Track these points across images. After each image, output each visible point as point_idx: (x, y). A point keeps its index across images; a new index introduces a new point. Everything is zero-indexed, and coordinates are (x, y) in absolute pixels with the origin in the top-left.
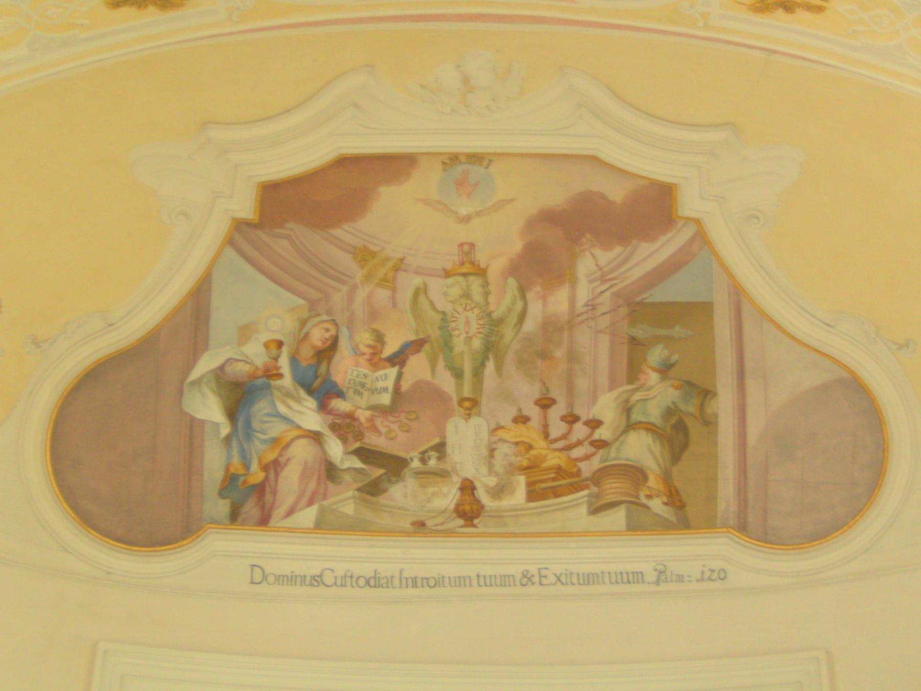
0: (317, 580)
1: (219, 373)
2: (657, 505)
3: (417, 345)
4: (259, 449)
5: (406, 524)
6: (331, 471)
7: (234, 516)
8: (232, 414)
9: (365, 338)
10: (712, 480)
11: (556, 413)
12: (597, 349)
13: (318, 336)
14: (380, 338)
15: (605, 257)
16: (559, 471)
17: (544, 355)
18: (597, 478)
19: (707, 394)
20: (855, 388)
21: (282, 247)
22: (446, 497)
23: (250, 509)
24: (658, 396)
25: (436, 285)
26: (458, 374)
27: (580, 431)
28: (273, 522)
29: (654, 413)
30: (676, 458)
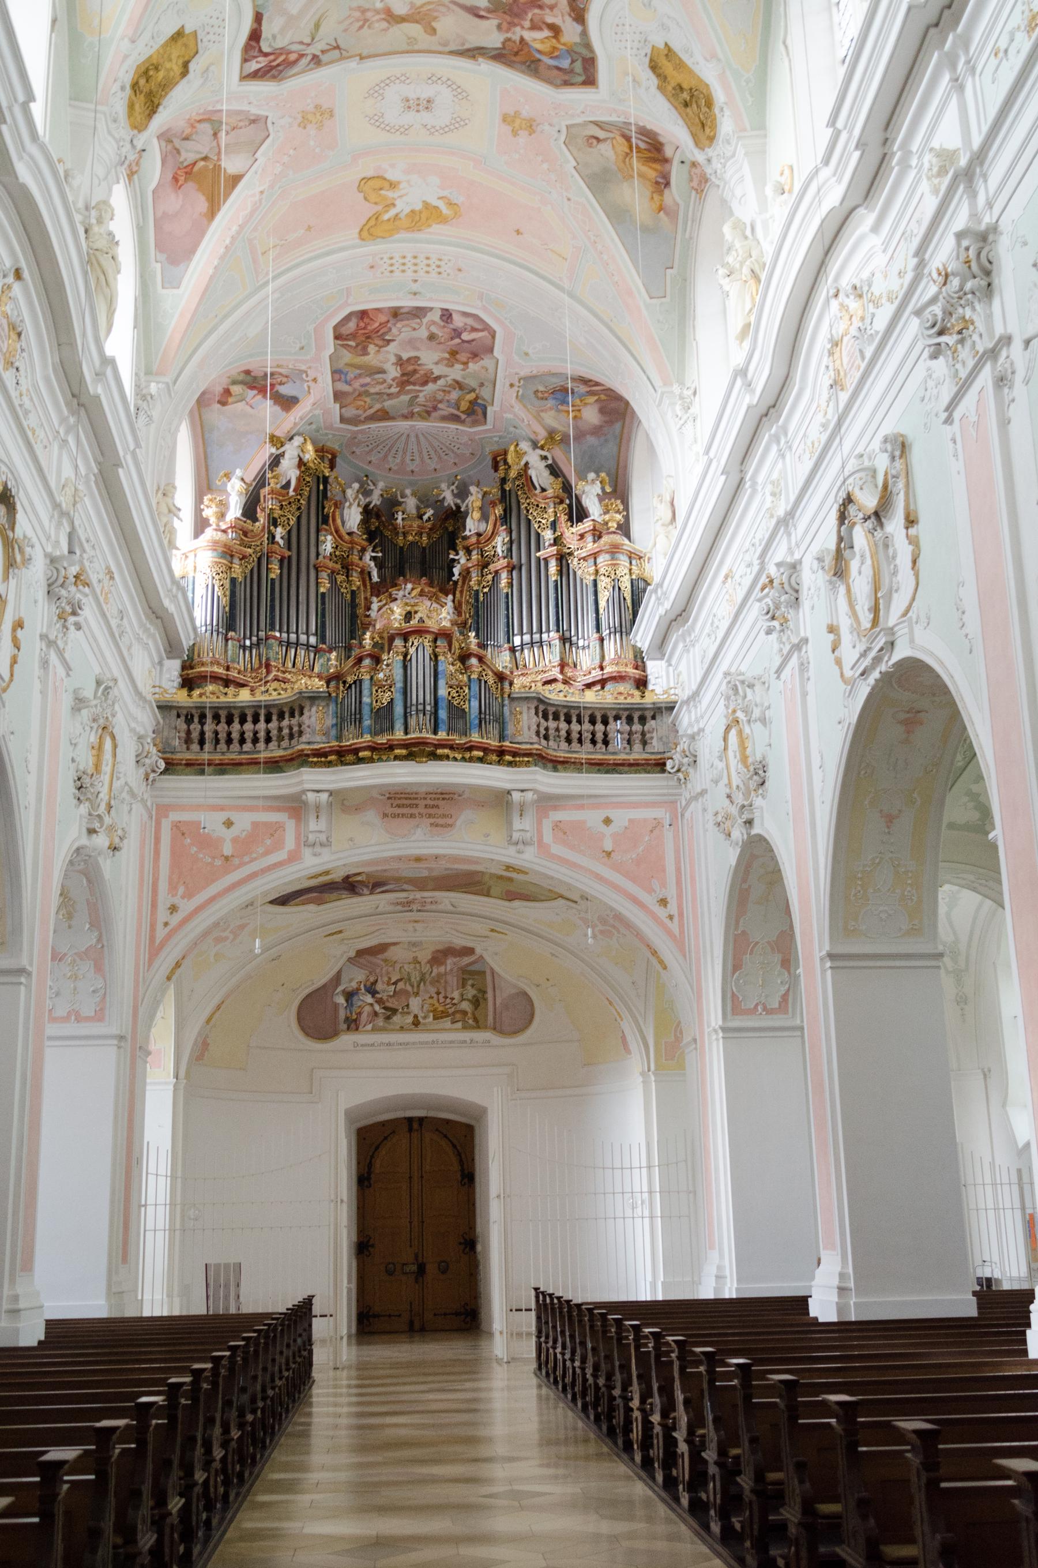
0: (373, 1045)
1: (343, 991)
2: (471, 1021)
3: (401, 980)
4: (355, 1009)
5: (398, 1027)
6: (376, 1014)
7: (348, 1029)
8: (347, 1001)
9: (386, 979)
10: (487, 1016)
11: (441, 996)
12: (453, 981)
13: (372, 979)
14: (390, 979)
15: (455, 960)
16: (442, 1012)
17: (437, 981)
18: (454, 1013)
19: (485, 992)
20: (526, 994)
21: (361, 960)
22: (410, 1019)
23: (353, 1025)
24: (471, 992)
25: (406, 966)
26: (413, 986)
27: (448, 1001)
28: (360, 1029)
29: (470, 997)
30: (476, 1009)
